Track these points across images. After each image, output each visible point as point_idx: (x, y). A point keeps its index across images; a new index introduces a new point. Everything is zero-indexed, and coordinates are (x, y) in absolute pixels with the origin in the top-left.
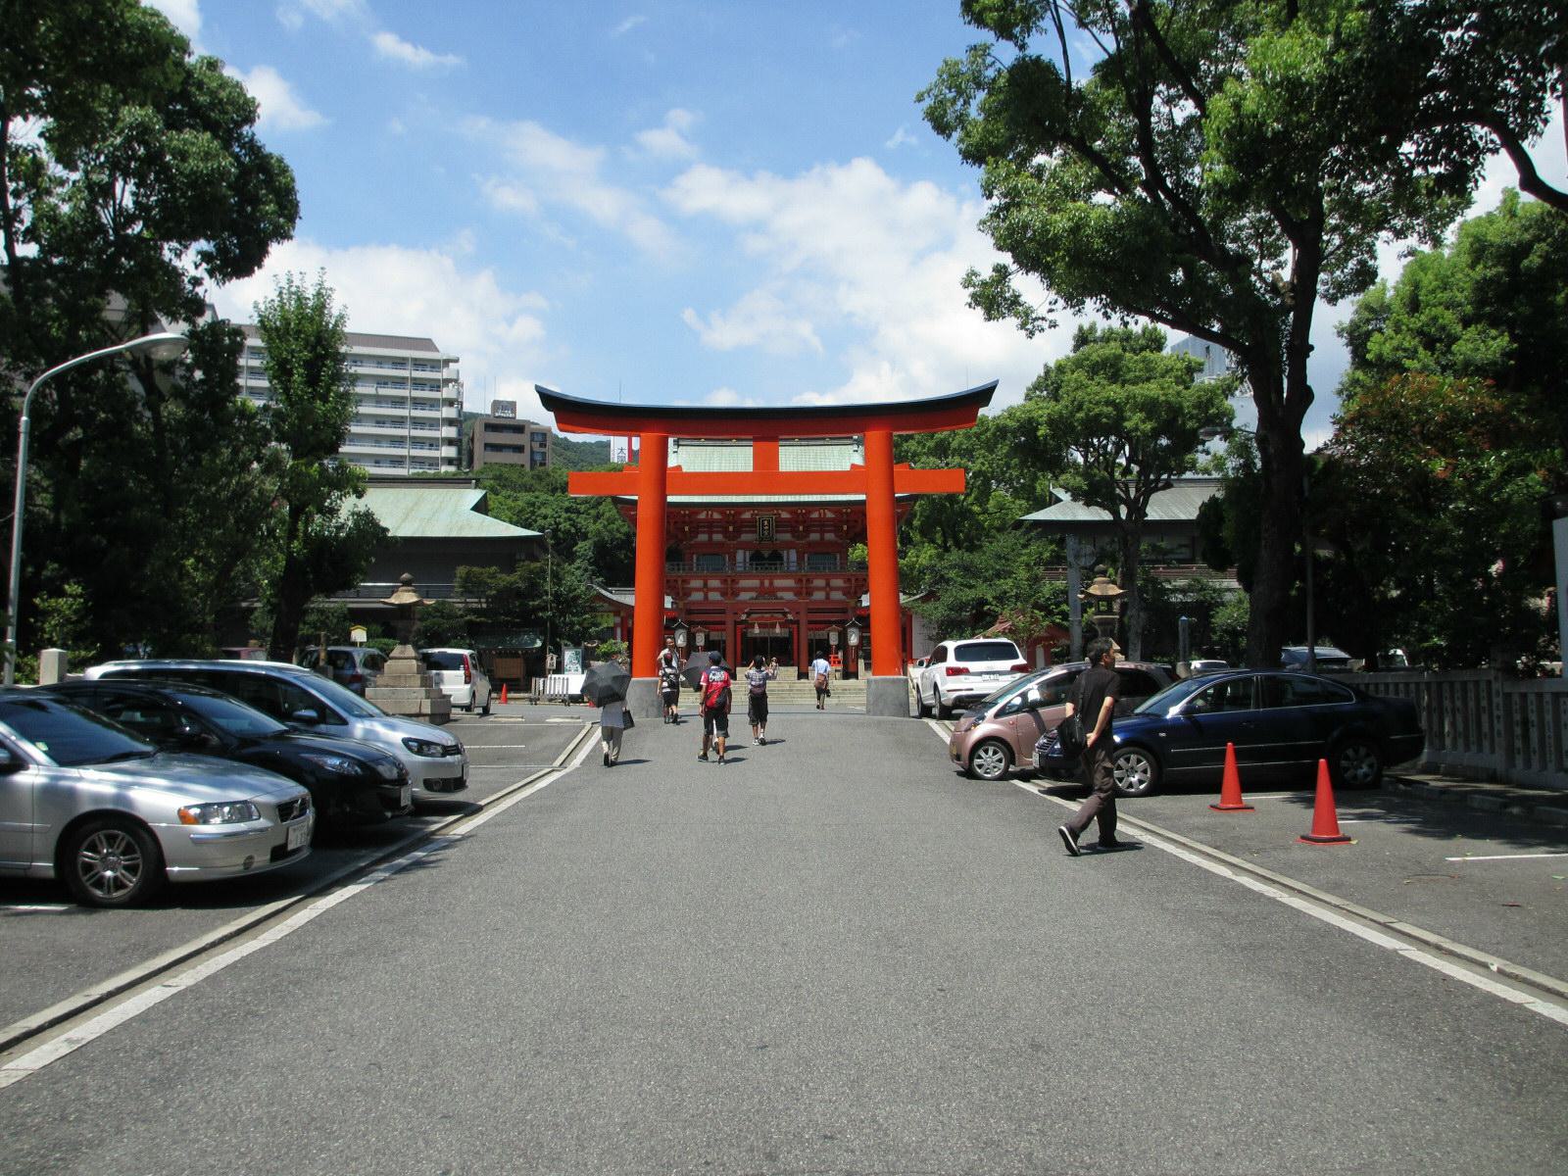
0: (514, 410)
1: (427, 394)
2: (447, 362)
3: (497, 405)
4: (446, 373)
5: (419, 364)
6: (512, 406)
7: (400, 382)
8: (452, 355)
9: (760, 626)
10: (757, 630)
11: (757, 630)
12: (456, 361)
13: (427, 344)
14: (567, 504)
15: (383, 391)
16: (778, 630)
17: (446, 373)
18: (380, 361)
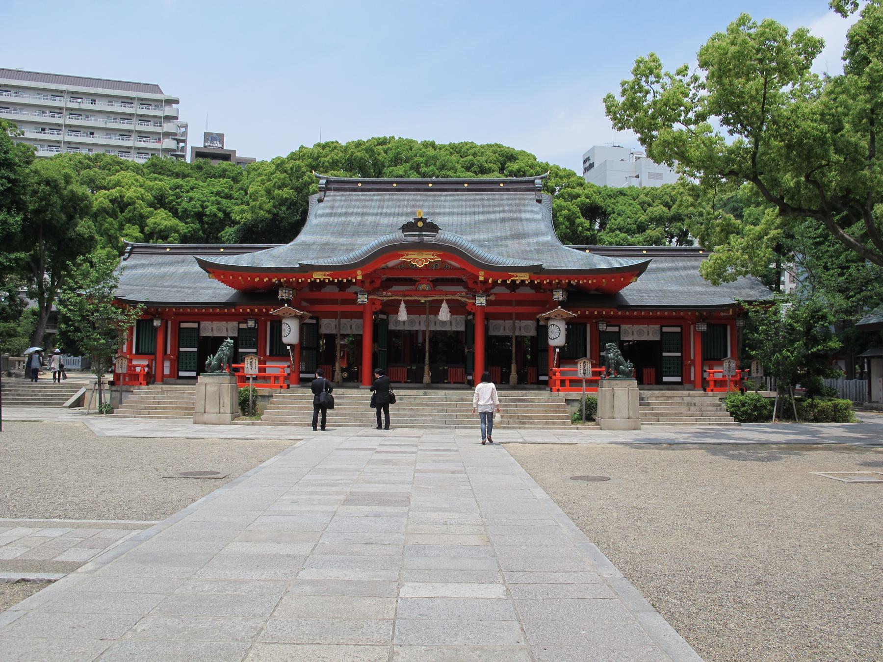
0: (222, 142)
1: (151, 128)
2: (170, 102)
3: (208, 136)
4: (168, 111)
5: (144, 102)
6: (220, 137)
7: (128, 117)
8: (173, 96)
9: (414, 308)
10: (403, 315)
11: (403, 315)
12: (177, 102)
13: (155, 88)
14: (218, 188)
15: (110, 125)
16: (444, 314)
17: (168, 111)
18: (111, 98)
